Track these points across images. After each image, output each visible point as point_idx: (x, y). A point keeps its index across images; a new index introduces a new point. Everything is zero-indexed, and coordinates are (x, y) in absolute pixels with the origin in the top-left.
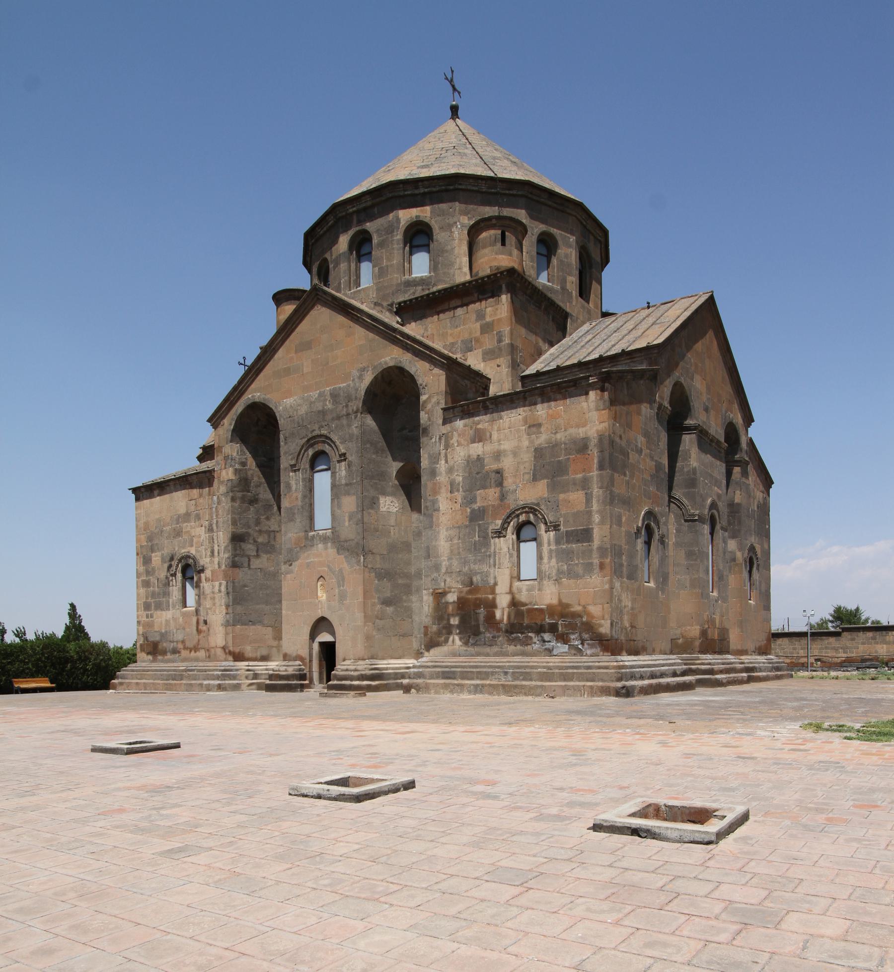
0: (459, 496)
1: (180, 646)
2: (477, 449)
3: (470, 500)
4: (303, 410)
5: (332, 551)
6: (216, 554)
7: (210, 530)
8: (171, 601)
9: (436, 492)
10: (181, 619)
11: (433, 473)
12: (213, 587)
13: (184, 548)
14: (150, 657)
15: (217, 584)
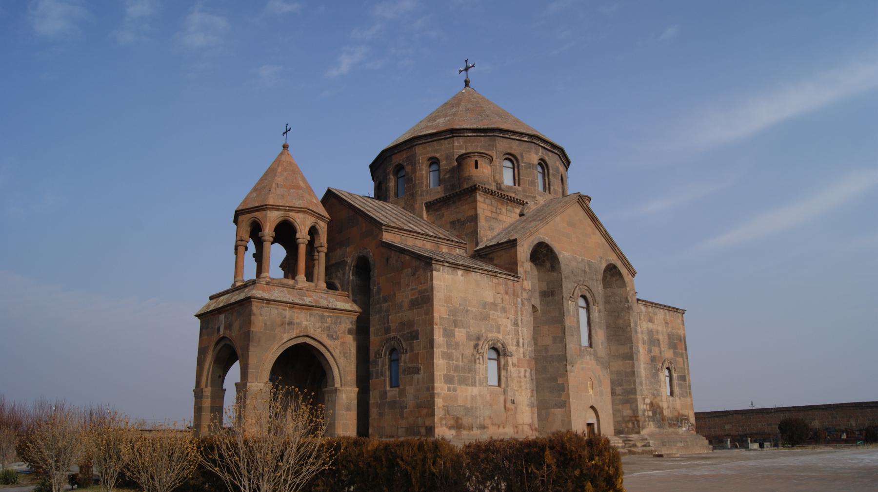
0: (646, 346)
1: (488, 422)
2: (650, 326)
3: (650, 351)
4: (574, 264)
5: (594, 362)
6: (521, 344)
7: (516, 324)
8: (477, 377)
9: (638, 342)
10: (488, 397)
11: (636, 332)
12: (519, 372)
13: (491, 332)
14: (453, 432)
15: (522, 370)
